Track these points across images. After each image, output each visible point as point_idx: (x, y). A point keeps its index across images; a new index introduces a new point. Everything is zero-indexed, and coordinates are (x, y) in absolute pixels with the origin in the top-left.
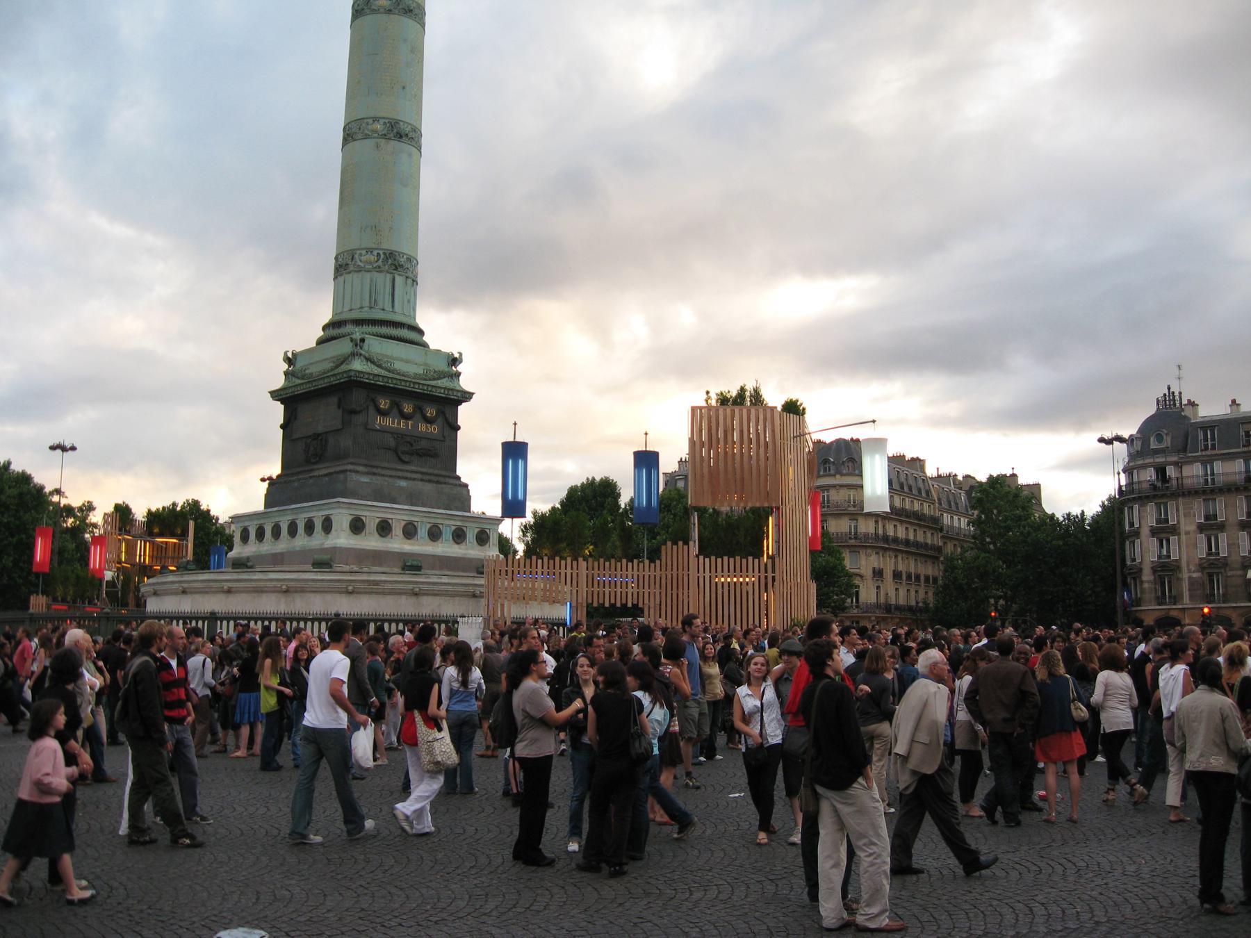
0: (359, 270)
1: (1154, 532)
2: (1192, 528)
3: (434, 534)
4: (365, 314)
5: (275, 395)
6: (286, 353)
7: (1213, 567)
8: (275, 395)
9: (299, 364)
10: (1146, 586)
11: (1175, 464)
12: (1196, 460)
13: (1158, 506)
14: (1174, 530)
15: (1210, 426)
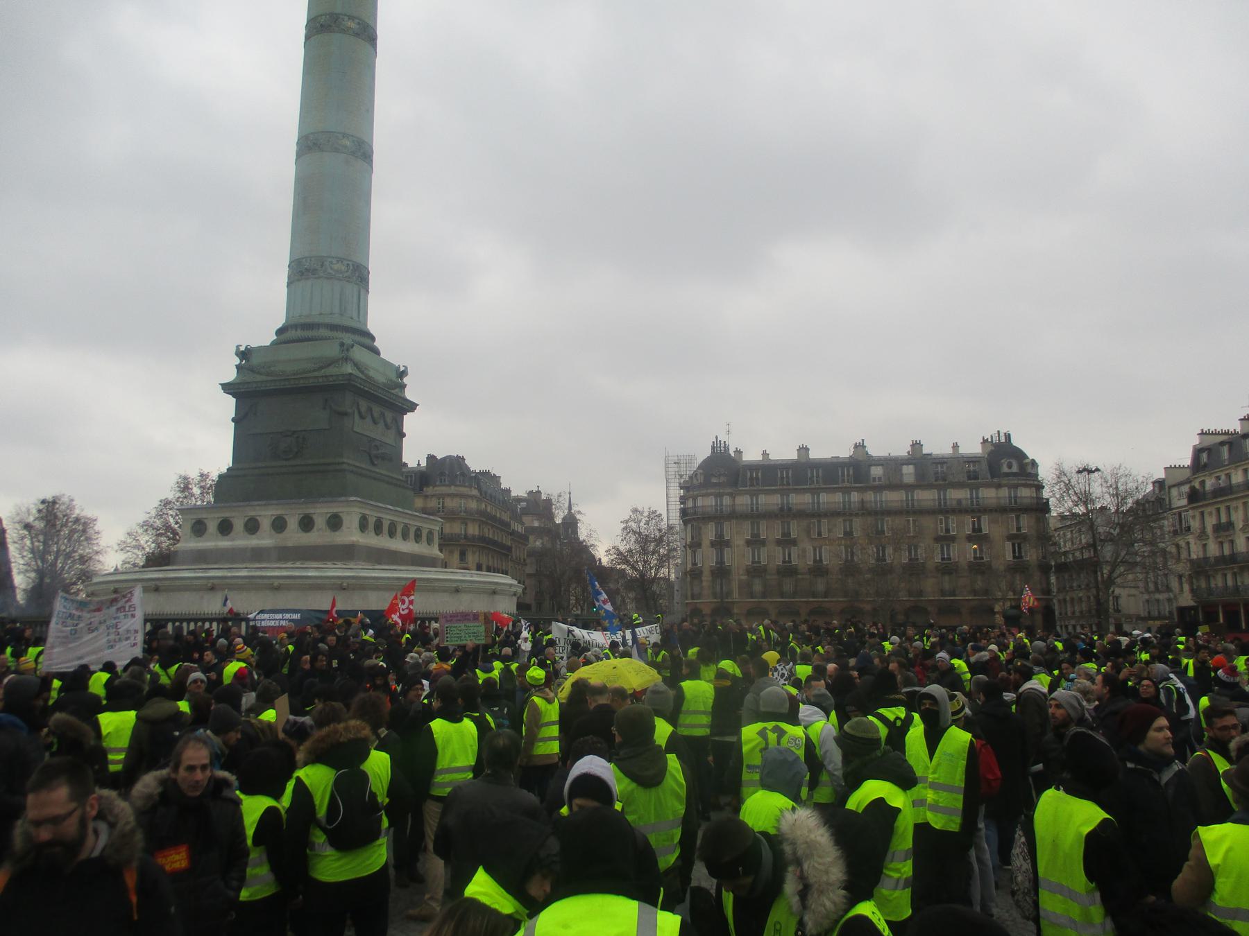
0: (330, 277)
1: (713, 544)
2: (742, 542)
3: (252, 527)
4: (336, 320)
5: (227, 388)
6: (238, 347)
7: (756, 571)
8: (227, 388)
9: (255, 361)
10: (704, 584)
11: (731, 495)
12: (746, 493)
13: (752, 524)
14: (727, 544)
15: (753, 467)
